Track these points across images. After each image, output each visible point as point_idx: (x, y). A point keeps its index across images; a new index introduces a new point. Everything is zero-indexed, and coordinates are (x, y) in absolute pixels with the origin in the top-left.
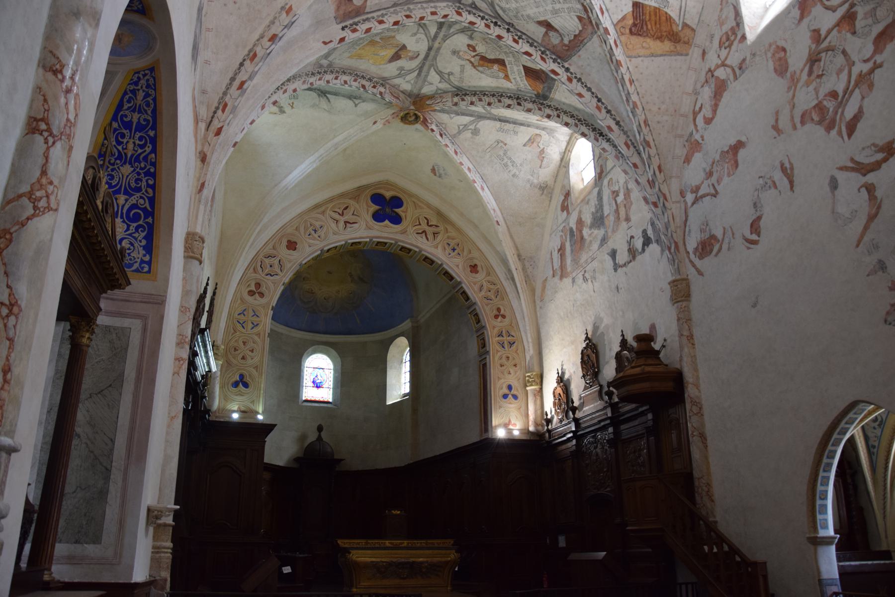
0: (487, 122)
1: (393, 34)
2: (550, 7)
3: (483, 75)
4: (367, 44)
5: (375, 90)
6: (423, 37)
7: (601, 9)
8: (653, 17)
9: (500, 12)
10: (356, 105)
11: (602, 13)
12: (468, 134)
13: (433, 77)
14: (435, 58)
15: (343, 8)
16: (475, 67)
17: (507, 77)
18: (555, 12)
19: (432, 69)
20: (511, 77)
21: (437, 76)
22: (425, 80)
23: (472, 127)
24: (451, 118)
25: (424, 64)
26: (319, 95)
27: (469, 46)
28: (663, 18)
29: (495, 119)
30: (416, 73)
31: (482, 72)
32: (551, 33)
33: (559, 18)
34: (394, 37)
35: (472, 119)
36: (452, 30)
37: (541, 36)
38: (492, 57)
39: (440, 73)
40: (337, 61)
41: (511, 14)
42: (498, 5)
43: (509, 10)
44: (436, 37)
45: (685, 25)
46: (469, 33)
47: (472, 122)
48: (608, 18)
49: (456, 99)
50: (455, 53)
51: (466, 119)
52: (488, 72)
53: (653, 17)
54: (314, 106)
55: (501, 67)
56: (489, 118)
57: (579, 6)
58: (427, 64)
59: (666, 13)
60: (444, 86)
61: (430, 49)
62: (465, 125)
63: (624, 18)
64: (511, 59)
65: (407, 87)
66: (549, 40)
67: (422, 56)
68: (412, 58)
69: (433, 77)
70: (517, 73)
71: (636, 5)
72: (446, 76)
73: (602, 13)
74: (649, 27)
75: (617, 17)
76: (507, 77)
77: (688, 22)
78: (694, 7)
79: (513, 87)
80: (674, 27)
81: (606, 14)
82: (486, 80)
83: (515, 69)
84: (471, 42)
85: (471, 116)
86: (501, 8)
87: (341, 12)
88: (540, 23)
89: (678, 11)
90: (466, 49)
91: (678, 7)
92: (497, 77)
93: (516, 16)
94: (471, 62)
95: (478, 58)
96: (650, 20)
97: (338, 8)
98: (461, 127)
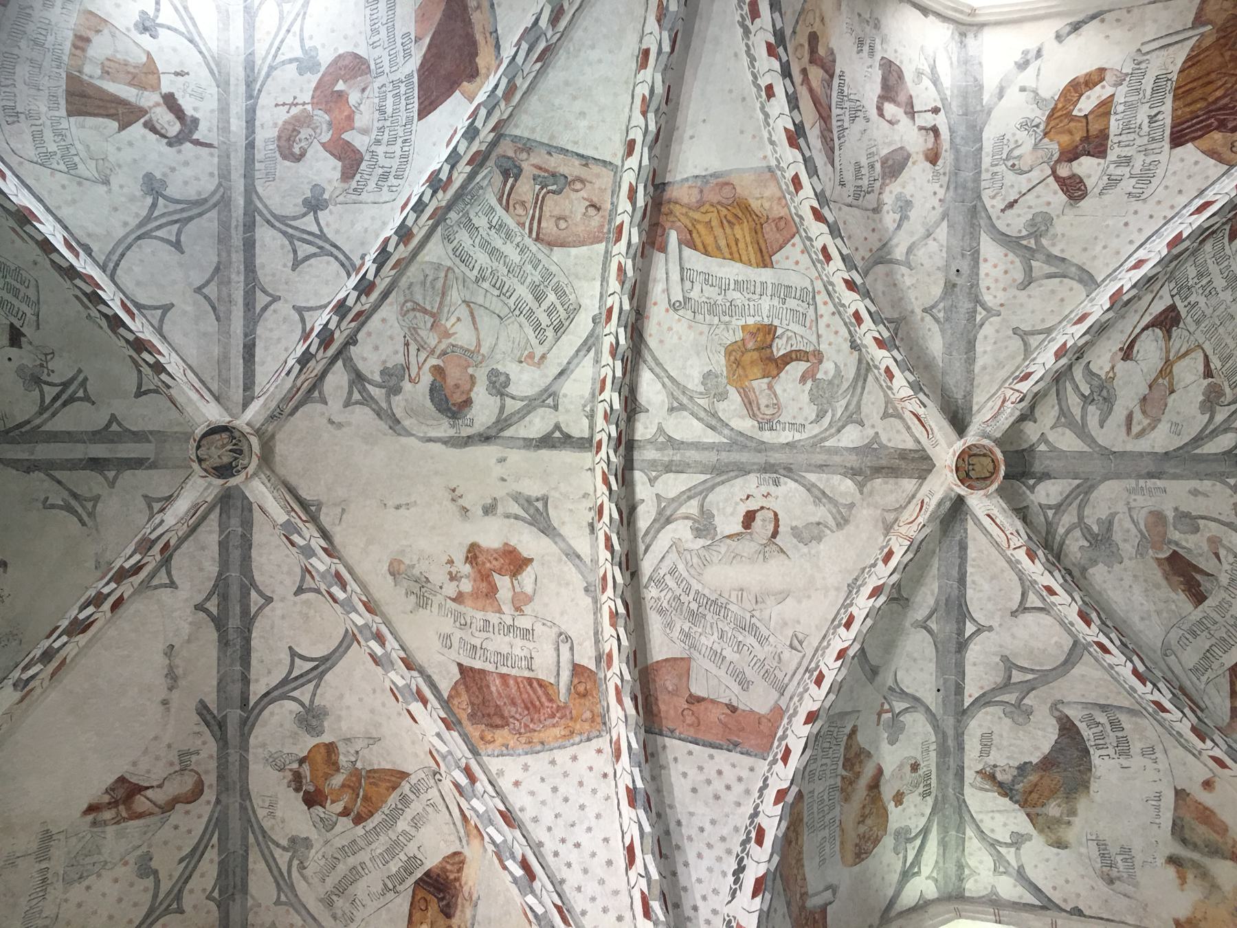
7: (1199, 210)
8: (1196, 94)
11: (1207, 204)
28: (1193, 72)
45: (1198, 21)
48: (1217, 187)
53: (1196, 94)
57: (1208, 246)
59: (1180, 72)
63: (1212, 153)
71: (1177, 140)
73: (1207, 204)
74: (1219, 93)
75: (1213, 168)
77: (1192, 16)
78: (1155, 21)
80: (1208, 42)
81: (1209, 196)
89: (1171, 49)
91: (1163, 53)
96: (1206, 100)
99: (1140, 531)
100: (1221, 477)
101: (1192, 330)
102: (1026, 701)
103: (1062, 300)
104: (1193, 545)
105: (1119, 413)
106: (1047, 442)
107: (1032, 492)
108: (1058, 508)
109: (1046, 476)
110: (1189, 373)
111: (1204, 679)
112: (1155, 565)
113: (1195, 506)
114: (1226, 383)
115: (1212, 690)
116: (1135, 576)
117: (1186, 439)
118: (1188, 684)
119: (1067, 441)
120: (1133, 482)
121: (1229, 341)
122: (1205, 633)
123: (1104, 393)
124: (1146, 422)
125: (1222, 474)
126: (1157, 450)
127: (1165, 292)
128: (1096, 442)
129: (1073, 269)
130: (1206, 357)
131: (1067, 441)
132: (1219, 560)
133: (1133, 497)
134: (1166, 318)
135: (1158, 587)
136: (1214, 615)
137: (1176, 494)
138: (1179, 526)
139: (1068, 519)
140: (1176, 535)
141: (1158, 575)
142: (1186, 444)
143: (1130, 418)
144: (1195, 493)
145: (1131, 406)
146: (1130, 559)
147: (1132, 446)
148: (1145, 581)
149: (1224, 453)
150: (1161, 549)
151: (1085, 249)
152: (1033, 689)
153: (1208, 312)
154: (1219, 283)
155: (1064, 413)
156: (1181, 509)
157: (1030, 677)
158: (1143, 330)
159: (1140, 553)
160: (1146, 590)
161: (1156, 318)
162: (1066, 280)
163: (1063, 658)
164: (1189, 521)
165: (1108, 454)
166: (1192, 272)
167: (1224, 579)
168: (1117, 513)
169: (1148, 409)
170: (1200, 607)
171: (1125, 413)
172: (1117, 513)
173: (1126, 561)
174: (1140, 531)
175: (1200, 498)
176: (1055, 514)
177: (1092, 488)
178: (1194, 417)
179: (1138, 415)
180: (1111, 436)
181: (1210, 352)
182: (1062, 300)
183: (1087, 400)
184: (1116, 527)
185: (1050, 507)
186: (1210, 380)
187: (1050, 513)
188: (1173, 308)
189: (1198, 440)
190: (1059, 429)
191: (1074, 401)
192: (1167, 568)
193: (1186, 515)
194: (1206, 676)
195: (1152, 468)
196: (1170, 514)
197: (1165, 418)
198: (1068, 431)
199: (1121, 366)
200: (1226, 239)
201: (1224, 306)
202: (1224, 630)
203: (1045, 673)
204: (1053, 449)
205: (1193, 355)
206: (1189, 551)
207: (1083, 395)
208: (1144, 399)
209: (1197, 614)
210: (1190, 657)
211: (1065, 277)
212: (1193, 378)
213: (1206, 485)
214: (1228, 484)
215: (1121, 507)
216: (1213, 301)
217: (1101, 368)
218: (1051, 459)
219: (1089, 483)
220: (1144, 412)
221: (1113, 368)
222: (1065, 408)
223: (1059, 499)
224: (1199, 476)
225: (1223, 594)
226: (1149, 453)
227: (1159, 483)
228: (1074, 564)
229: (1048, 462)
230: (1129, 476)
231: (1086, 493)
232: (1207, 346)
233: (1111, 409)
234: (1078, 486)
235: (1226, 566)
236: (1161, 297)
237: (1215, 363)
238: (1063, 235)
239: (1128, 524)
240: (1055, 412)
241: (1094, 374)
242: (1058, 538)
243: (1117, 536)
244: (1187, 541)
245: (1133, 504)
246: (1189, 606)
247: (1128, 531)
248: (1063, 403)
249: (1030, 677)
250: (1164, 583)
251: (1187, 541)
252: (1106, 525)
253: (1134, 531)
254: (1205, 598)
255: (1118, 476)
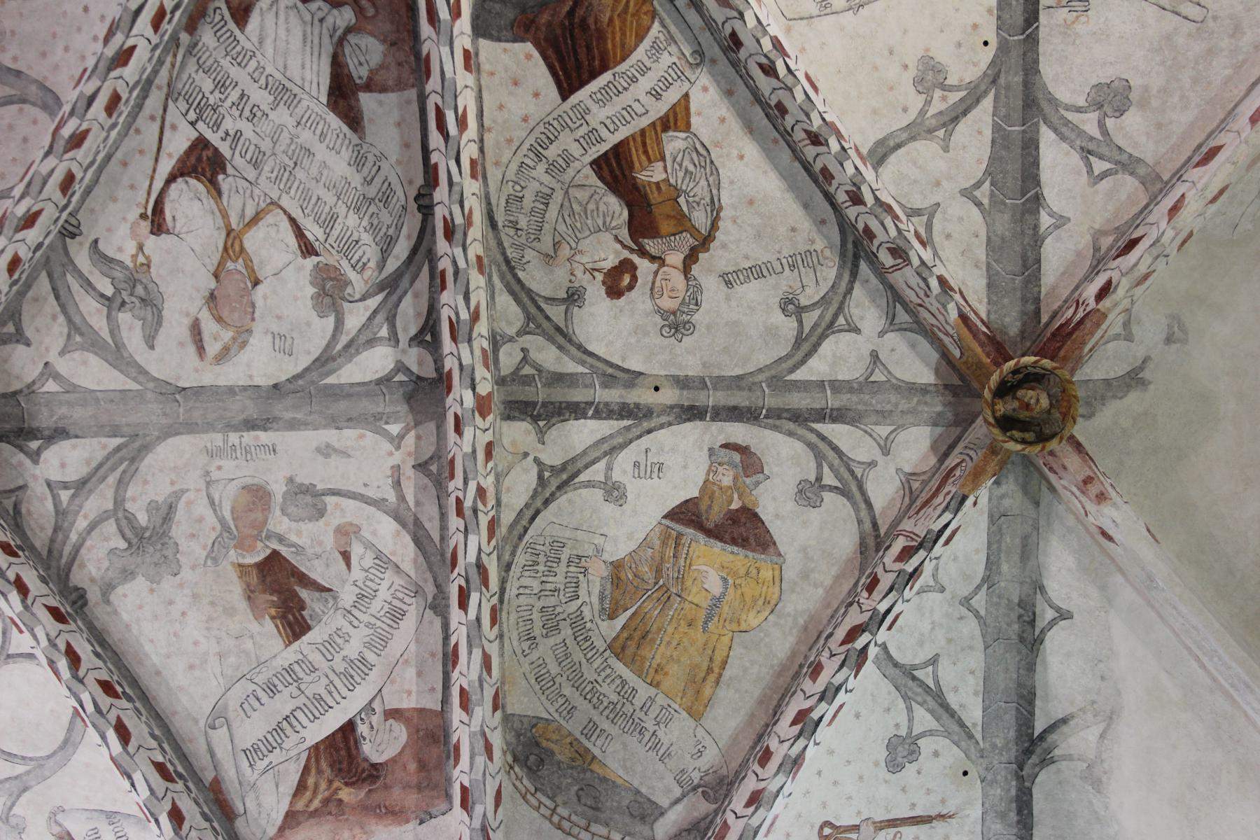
0: (1048, 69)
1: (598, 572)
2: (282, 116)
3: (725, 199)
4: (633, 662)
5: (886, 581)
6: (624, 460)
9: (402, 250)
10: (1064, 615)
12: (1132, 130)
13: (838, 359)
14: (737, 382)
15: (397, 795)
16: (705, 242)
17: (676, 119)
18: (283, 93)
19: (798, 375)
20: (659, 109)
21: (827, 347)
22: (866, 385)
23: (1089, 123)
24: (1061, 221)
25: (776, 414)
26: (1046, 761)
27: (614, 291)
29: (1032, 41)
30: (826, 428)
31: (716, 210)
32: (359, 73)
33: (295, 73)
34: (617, 566)
35: (1047, 137)
36: (571, 367)
37: (391, 98)
38: (615, 208)
39: (806, 345)
40: (711, 757)
41: (386, 218)
42: (382, 264)
43: (373, 228)
44: (625, 411)
46: (556, 313)
47: (1065, 131)
49: (886, 259)
50: (677, 324)
51: (1056, 159)
52: (701, 190)
54: (1094, 778)
55: (636, 156)
56: (1031, 68)
57: (207, 37)
58: (772, 401)
60: (865, 309)
61: (692, 413)
62: (1086, 153)
64: (567, 142)
65: (915, 446)
66: (382, 66)
67: (738, 432)
68: (748, 461)
69: (838, 359)
70: (626, 98)
72: (810, 319)
76: (676, 119)
79: (704, 78)
82: (746, 182)
83: (599, 114)
84: (595, 290)
85: (1030, 146)
86: (385, 254)
87: (411, 799)
88: (354, 120)
90: (638, 299)
92: (703, 155)
93: (386, 200)
94: (691, 258)
95: (651, 245)
97: (395, 814)
98: (1099, 166)
99: (222, 521)
100: (374, 422)
101: (251, 177)
102: (15, 810)
103: (25, 140)
104: (308, 541)
105: (175, 326)
106: (57, 377)
107: (36, 462)
108: (81, 486)
109: (59, 433)
110: (271, 246)
111: (261, 765)
112: (233, 575)
113: (321, 474)
114: (344, 263)
115: (267, 784)
116: (195, 597)
117: (305, 362)
118: (229, 773)
119: (92, 373)
120: (217, 439)
121: (322, 192)
122: (293, 689)
123: (140, 290)
124: (227, 335)
125: (378, 417)
126: (259, 381)
127: (173, 114)
128: (147, 373)
129: (33, 88)
130: (293, 221)
131: (92, 373)
132: (348, 565)
133: (218, 462)
134: (199, 159)
135: (230, 611)
136: (316, 658)
137: (293, 454)
138: (292, 509)
139: (98, 502)
140: (279, 523)
141: (235, 591)
142: (307, 370)
143: (196, 330)
144: (326, 451)
145: (193, 311)
146: (193, 567)
147: (211, 376)
148: (212, 604)
149: (379, 382)
150: (251, 549)
151: (44, 55)
152: (25, 789)
153: (266, 145)
154: (260, 97)
155: (76, 327)
156: (298, 480)
157: (20, 769)
158: (171, 179)
159: (213, 557)
160: (210, 619)
161: (183, 160)
162: (27, 107)
163: (61, 736)
164: (309, 499)
165: (172, 392)
166: (207, 85)
167: (347, 596)
168: (183, 491)
169: (225, 313)
170: (296, 645)
171: (187, 322)
172: (183, 491)
173: (186, 574)
174: (222, 521)
175: (335, 460)
176: (74, 496)
177: (146, 448)
178: (308, 324)
179: (209, 326)
180: (171, 360)
181: (297, 214)
182: (25, 140)
183: (111, 304)
184: (180, 514)
185: (65, 485)
186: (315, 259)
187: (65, 495)
188: (201, 144)
189: (325, 361)
190: (77, 355)
191: (91, 310)
192: (254, 579)
193: (307, 490)
194: (266, 761)
195: (252, 411)
196: (278, 489)
197: (258, 327)
198: (93, 360)
199: (152, 243)
200: (232, 25)
201: (285, 134)
202: (324, 681)
203: (40, 762)
204: (72, 388)
205: (269, 219)
206: (299, 549)
207: (102, 296)
208: (212, 296)
209: (289, 655)
210: (252, 730)
211: (24, 101)
212: (287, 257)
213: (347, 437)
214: (387, 435)
215: (193, 481)
216: (265, 127)
217: (120, 249)
218: (70, 404)
219: (137, 444)
220: (219, 319)
221: (141, 247)
222: (77, 320)
223: (84, 471)
224: (335, 423)
225: (340, 621)
226: (245, 388)
227: (264, 437)
228: (92, 580)
229: (64, 410)
230: (210, 427)
231: (133, 460)
232: (285, 202)
233: (160, 317)
234: (118, 449)
235: (357, 574)
236: (174, 127)
237: (314, 232)
238: (13, 33)
239: (202, 508)
240: (60, 327)
241: (111, 260)
242: (74, 537)
243: (180, 530)
244: (299, 533)
245: (215, 475)
246: (276, 643)
247: (201, 520)
248: (71, 311)
249: (20, 769)
250: (243, 605)
251: (299, 533)
252: (164, 510)
253: (211, 520)
254: (309, 628)
255: (191, 428)
